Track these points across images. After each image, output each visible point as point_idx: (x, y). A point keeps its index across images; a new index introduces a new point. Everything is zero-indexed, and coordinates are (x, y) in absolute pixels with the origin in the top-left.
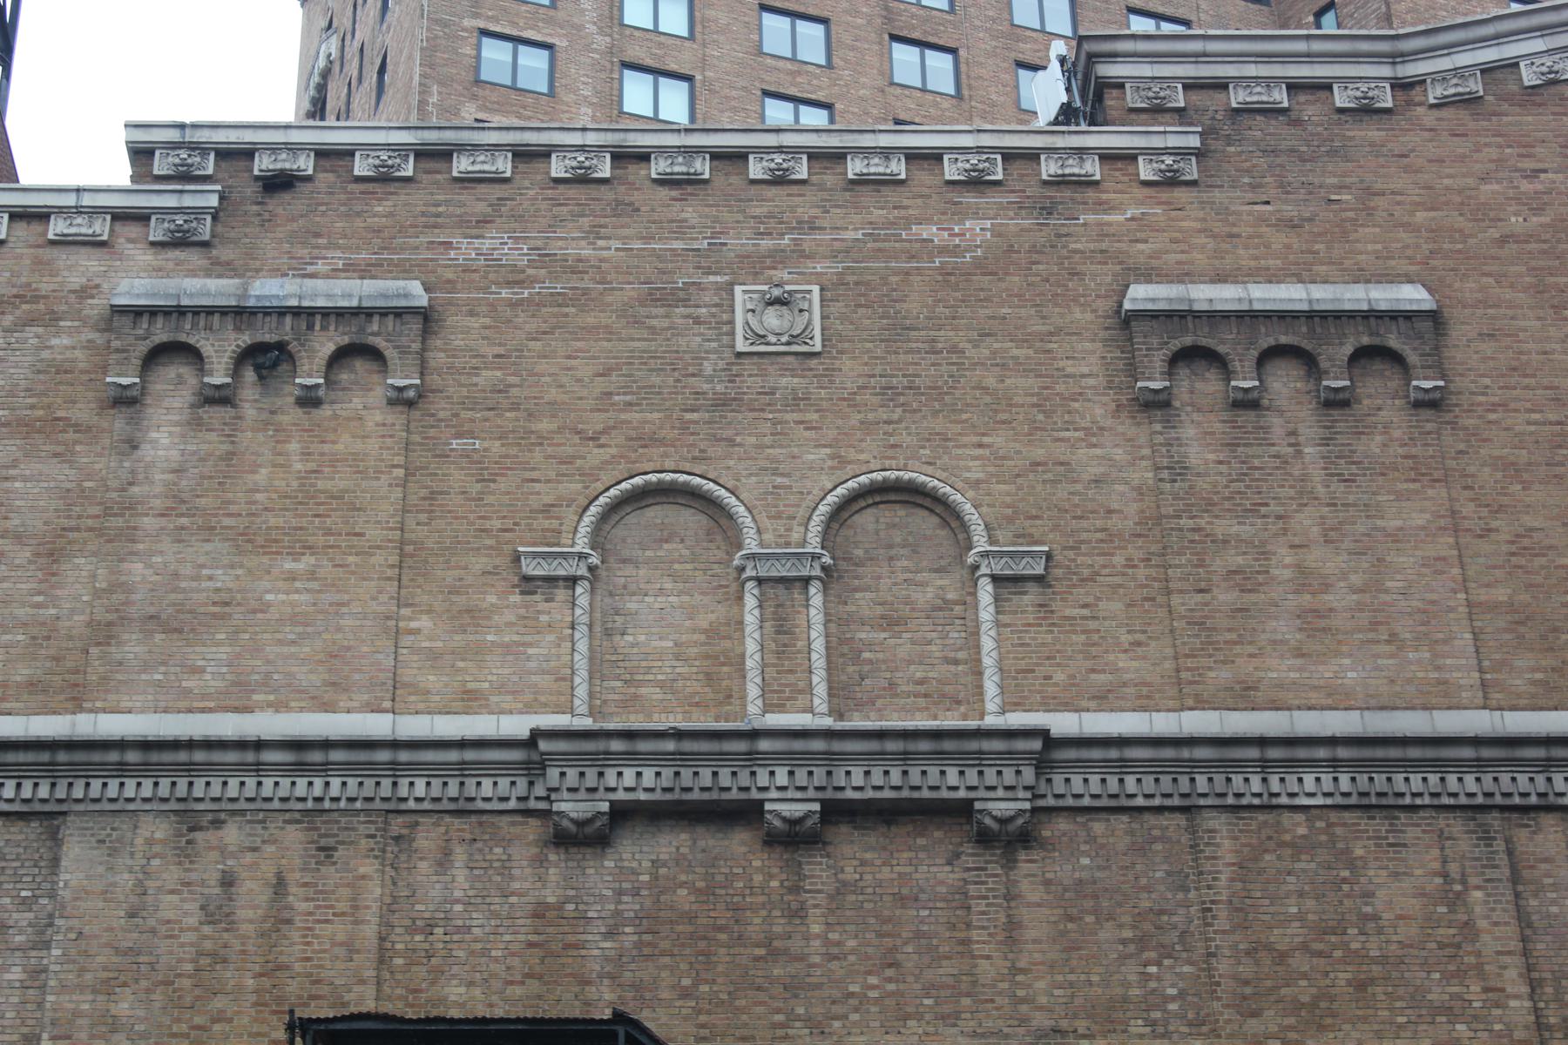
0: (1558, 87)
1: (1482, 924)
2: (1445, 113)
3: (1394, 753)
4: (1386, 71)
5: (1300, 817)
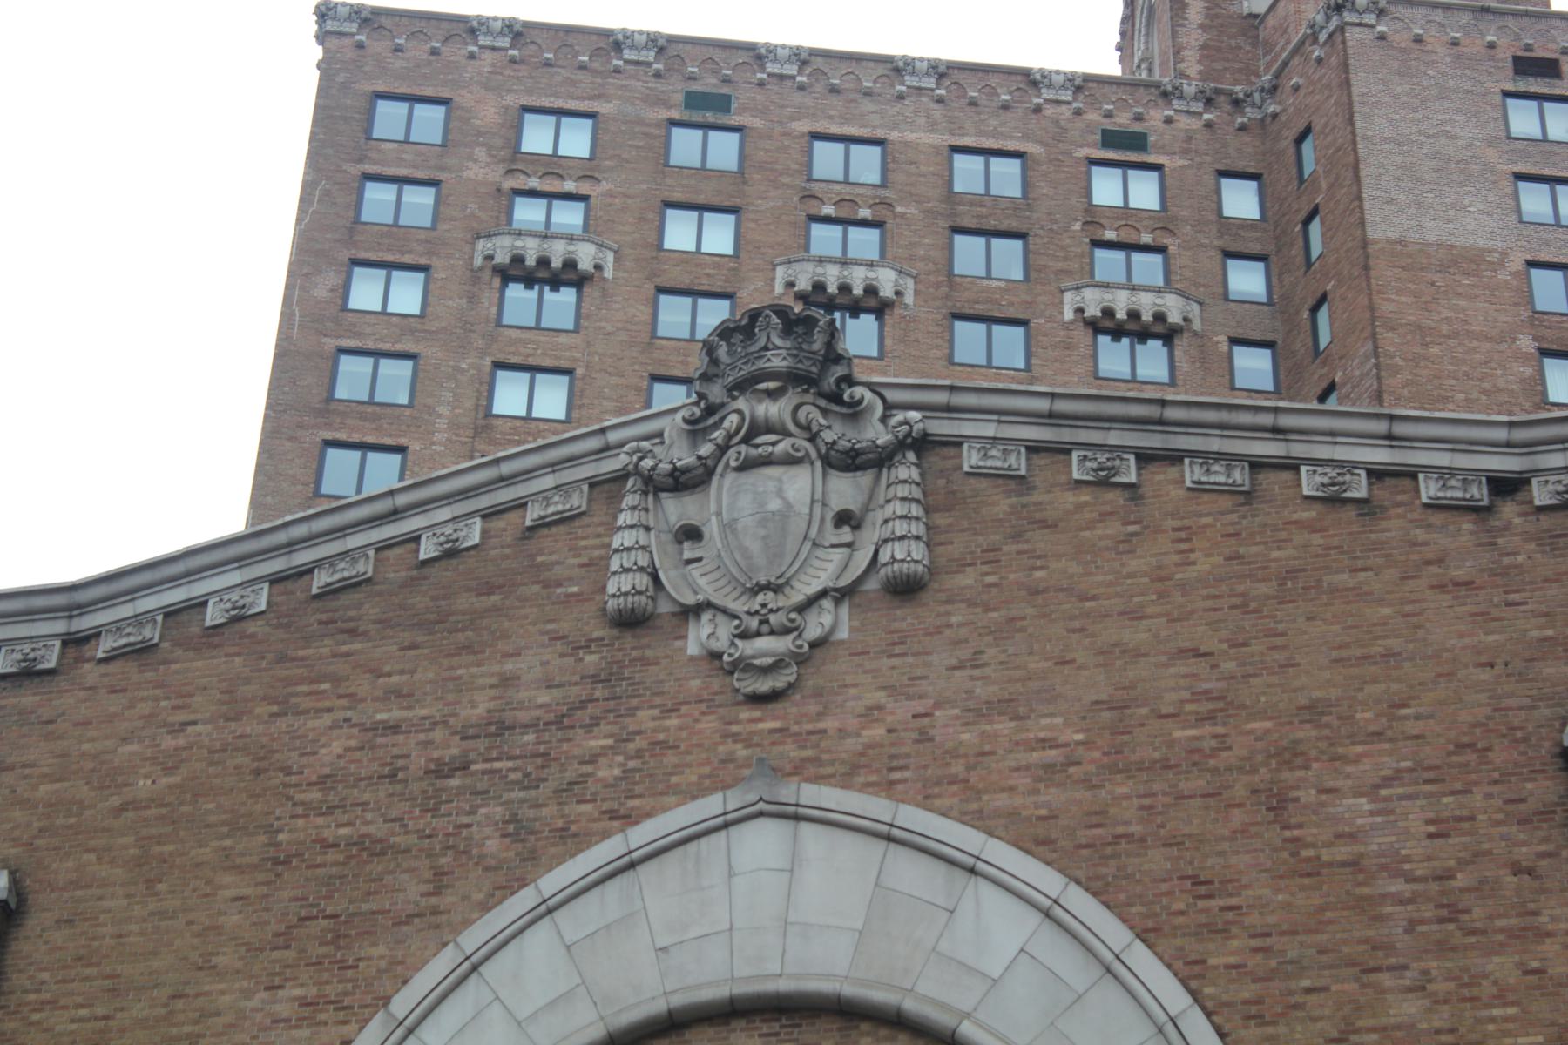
0: (243, 624)
2: (114, 667)
4: (60, 627)
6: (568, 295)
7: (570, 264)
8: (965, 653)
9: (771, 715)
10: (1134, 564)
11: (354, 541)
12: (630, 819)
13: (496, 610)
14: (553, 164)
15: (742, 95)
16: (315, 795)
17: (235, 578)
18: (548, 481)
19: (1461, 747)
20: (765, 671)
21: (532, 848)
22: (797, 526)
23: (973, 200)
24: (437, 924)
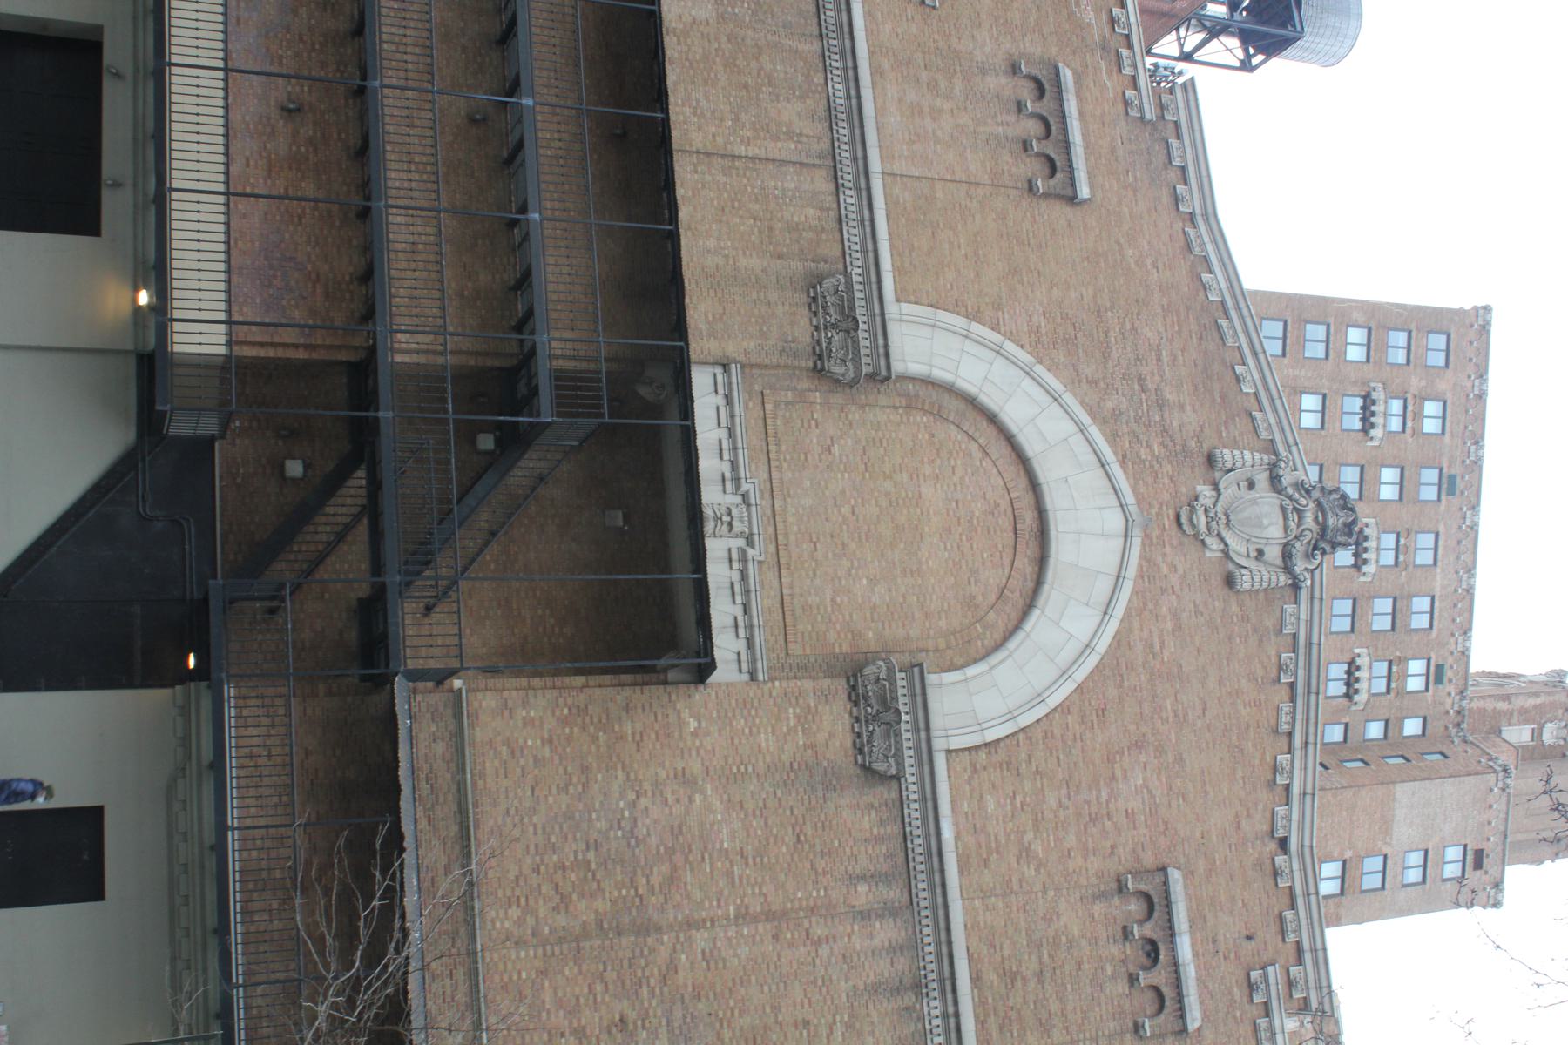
1: (779, 144)
2: (1181, 235)
3: (856, 123)
4: (1198, 211)
5: (822, 81)
6: (1358, 425)
7: (1373, 426)
8: (1201, 608)
9: (1173, 526)
10: (1244, 681)
11: (1242, 336)
12: (1123, 463)
13: (1214, 400)
14: (1419, 416)
15: (1455, 501)
16: (1128, 326)
17: (1223, 285)
18: (1272, 421)
19: (1166, 824)
20: (1191, 520)
21: (1109, 421)
22: (1256, 532)
23: (1409, 606)
24: (1074, 382)
